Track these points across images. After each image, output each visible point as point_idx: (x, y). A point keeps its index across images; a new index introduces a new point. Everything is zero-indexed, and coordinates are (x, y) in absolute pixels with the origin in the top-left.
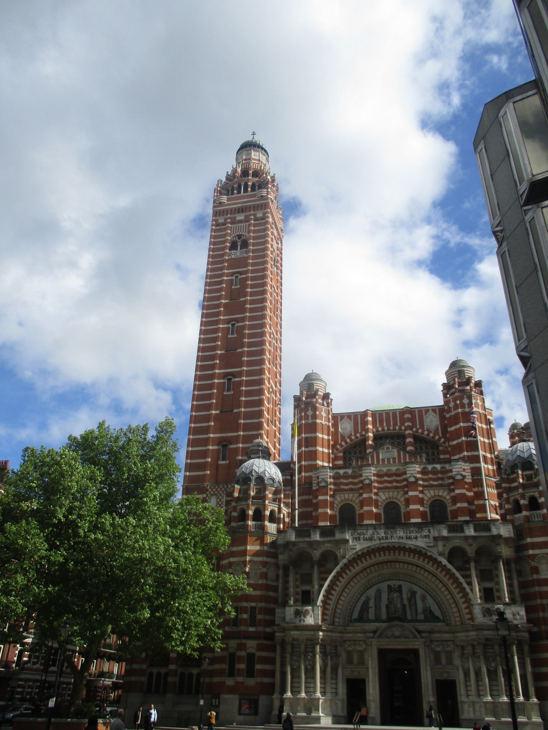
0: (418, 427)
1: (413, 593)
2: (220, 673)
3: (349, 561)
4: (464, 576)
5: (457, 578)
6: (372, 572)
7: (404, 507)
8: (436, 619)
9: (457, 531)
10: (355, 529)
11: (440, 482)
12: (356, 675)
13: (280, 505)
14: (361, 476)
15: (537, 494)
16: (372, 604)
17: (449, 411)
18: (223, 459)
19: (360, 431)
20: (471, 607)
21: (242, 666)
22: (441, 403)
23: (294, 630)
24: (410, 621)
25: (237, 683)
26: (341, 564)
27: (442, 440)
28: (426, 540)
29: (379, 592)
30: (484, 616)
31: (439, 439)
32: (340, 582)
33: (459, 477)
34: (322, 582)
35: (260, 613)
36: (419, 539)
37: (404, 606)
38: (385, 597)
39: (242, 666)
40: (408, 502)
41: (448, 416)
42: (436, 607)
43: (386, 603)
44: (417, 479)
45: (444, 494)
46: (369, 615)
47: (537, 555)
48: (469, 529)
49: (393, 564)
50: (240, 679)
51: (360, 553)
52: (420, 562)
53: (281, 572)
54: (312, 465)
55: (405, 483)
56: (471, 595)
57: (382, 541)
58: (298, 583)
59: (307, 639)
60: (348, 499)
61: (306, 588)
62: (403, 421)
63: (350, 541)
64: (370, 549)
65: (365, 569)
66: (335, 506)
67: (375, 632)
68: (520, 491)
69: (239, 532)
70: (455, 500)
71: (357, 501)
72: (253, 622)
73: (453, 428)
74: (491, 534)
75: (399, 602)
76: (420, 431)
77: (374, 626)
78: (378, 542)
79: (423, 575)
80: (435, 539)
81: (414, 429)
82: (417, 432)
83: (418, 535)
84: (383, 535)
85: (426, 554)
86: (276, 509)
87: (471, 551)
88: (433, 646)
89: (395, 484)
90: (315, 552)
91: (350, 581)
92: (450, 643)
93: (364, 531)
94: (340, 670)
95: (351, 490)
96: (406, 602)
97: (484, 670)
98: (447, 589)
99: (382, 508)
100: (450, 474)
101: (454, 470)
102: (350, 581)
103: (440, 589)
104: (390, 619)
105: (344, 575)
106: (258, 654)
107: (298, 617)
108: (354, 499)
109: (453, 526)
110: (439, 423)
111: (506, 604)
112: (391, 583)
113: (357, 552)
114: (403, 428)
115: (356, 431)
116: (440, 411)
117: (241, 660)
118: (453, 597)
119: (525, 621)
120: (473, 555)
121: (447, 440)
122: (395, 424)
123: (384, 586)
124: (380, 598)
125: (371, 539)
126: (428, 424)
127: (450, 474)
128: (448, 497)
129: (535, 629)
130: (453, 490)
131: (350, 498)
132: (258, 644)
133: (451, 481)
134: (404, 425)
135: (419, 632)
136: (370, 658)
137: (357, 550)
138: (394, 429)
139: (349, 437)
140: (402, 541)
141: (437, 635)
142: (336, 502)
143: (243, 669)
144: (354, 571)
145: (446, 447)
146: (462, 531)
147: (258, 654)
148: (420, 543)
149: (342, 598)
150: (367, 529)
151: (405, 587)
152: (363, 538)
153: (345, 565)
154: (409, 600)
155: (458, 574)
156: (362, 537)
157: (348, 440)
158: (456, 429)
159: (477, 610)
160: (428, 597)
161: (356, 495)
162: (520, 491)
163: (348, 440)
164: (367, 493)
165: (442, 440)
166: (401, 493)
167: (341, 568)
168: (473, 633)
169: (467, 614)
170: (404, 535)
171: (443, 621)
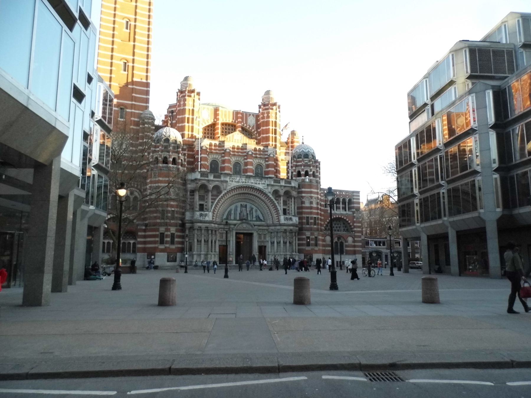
1: (252, 209)
2: (155, 242)
3: (227, 192)
4: (278, 203)
6: (235, 198)
7: (243, 166)
8: (261, 220)
9: (277, 183)
10: (231, 176)
11: (262, 156)
13: (185, 157)
14: (224, 146)
15: (309, 170)
16: (233, 212)
17: (263, 118)
18: (121, 118)
20: (279, 217)
21: (169, 239)
22: (258, 112)
23: (198, 222)
24: (250, 221)
25: (165, 247)
26: (223, 193)
27: (256, 132)
28: (264, 185)
29: (236, 207)
30: (285, 220)
31: (254, 132)
33: (272, 155)
35: (177, 213)
36: (260, 184)
37: (247, 214)
38: (239, 209)
39: (169, 239)
40: (246, 164)
41: (262, 120)
42: (262, 215)
43: (239, 212)
44: (252, 153)
45: (263, 162)
46: (231, 217)
47: (305, 196)
48: (282, 182)
49: (245, 195)
50: (167, 245)
51: (233, 188)
52: (259, 195)
53: (189, 193)
55: (245, 154)
57: (244, 184)
59: (206, 227)
60: (217, 159)
61: (202, 203)
63: (229, 182)
64: (237, 187)
65: (232, 196)
66: (208, 161)
67: (235, 225)
68: (303, 167)
69: (163, 170)
70: (268, 166)
71: (220, 160)
72: (173, 218)
73: (264, 128)
74: (291, 186)
75: (245, 212)
76: (245, 125)
77: (235, 222)
78: (241, 184)
79: (258, 201)
80: (268, 185)
81: (242, 124)
82: (243, 125)
83: (260, 183)
84: (244, 180)
85: (263, 191)
86: (183, 159)
87: (282, 192)
88: (259, 232)
89: (240, 154)
90: (210, 185)
92: (265, 231)
93: (235, 178)
94: (217, 241)
95: (217, 153)
96: (248, 212)
97: (282, 242)
98: (268, 208)
99: (232, 165)
100: (266, 153)
101: (269, 151)
104: (241, 220)
106: (176, 234)
107: (202, 217)
108: (219, 158)
109: (276, 180)
110: (255, 123)
111: (293, 216)
112: (242, 203)
113: (231, 188)
114: (237, 122)
116: (257, 116)
117: (167, 236)
119: (298, 223)
120: (283, 194)
121: (259, 134)
123: (239, 204)
124: (237, 210)
125: (238, 182)
126: (250, 122)
127: (266, 153)
128: (264, 164)
129: (300, 226)
130: (267, 161)
131: (217, 157)
132: (176, 229)
133: (266, 156)
135: (255, 226)
136: (231, 236)
137: (232, 186)
140: (252, 184)
141: (261, 227)
142: (209, 159)
143: (169, 241)
144: (228, 196)
145: (256, 136)
146: (279, 183)
147: (176, 234)
148: (261, 186)
149: (220, 209)
150: (237, 177)
151: (249, 205)
153: (225, 193)
154: (250, 212)
155: (276, 202)
156: (234, 180)
158: (266, 129)
159: (282, 218)
160: (258, 210)
161: (220, 156)
162: (303, 167)
164: (228, 157)
165: (256, 132)
166: (243, 159)
168: (278, 227)
169: (277, 219)
170: (254, 182)
171: (264, 222)
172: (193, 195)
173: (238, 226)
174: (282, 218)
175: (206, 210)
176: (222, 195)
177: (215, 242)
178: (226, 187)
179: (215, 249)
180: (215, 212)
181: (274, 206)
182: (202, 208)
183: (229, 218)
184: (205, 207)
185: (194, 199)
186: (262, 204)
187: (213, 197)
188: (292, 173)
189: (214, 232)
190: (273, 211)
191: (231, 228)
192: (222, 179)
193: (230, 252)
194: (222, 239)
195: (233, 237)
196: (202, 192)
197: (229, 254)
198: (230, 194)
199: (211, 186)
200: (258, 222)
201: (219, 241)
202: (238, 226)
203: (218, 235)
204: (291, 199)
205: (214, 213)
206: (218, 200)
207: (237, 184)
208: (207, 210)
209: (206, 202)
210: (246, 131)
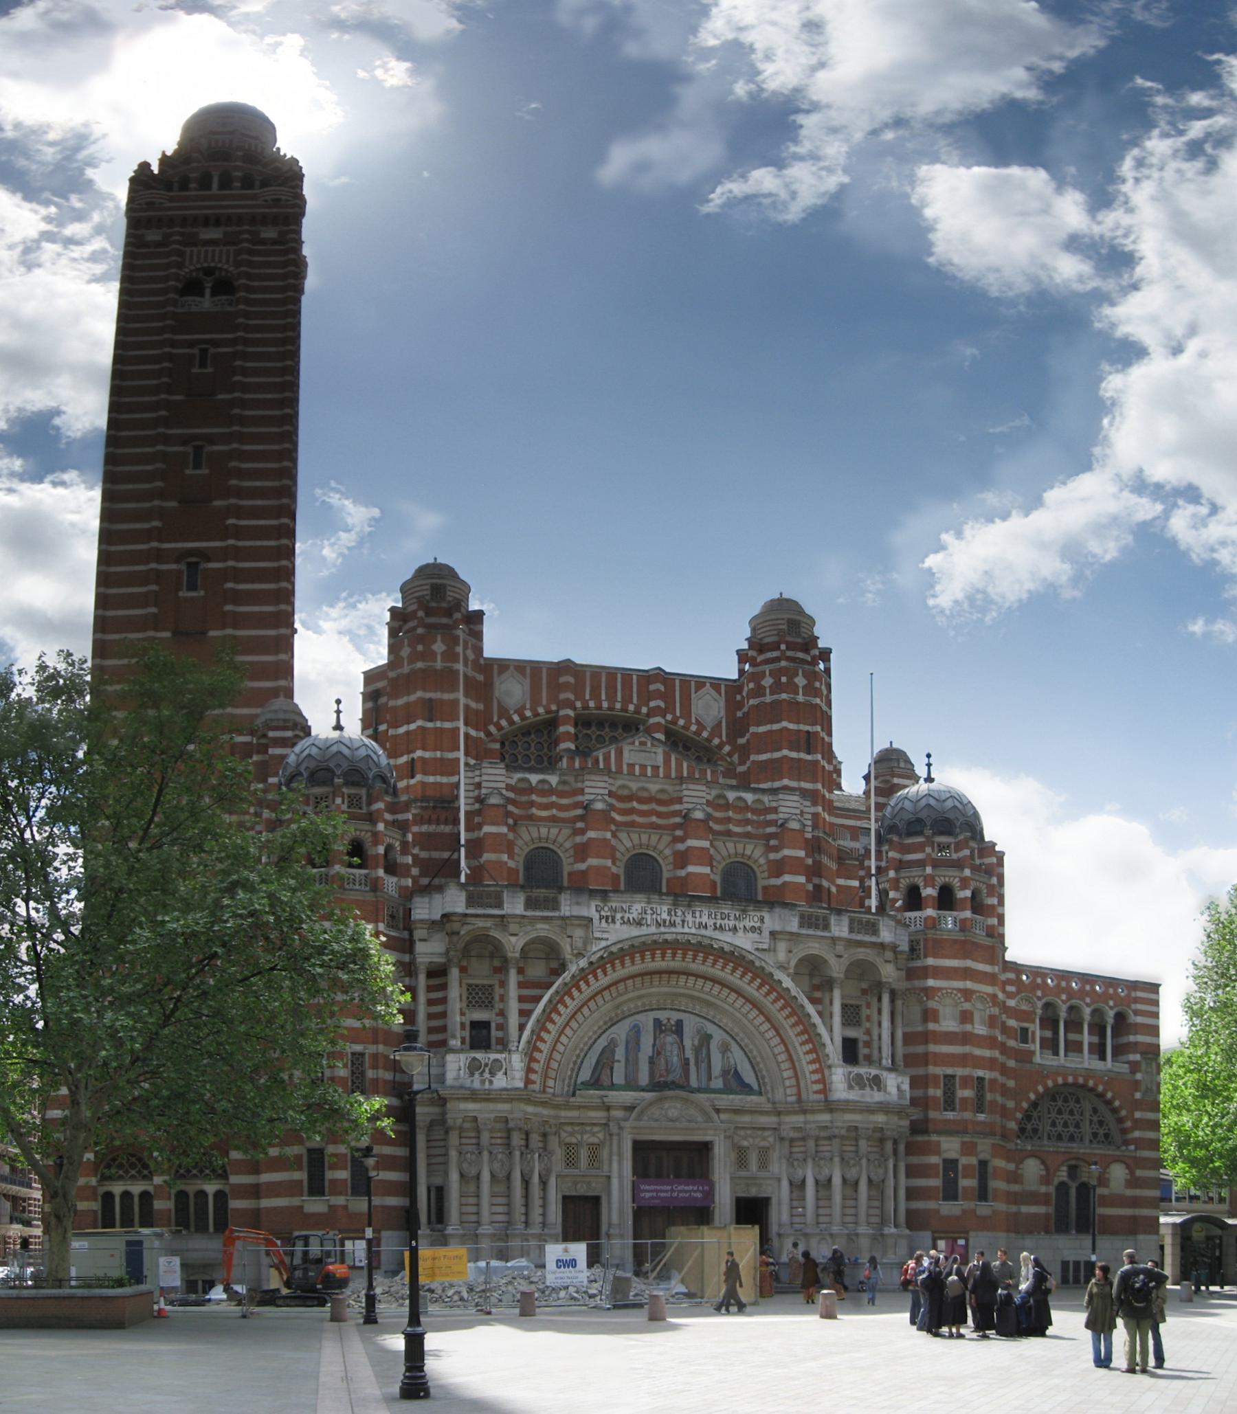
0: (678, 714)
3: (591, 963)
5: (809, 1015)
12: (582, 1190)
19: (544, 702)
26: (573, 969)
32: (566, 1007)
34: (527, 1006)
51: (614, 949)
54: (442, 759)
56: (830, 1049)
58: (464, 1004)
62: (646, 697)
65: (615, 983)
76: (681, 722)
78: (653, 929)
82: (674, 722)
90: (513, 939)
91: (582, 1007)
94: (552, 1181)
98: (779, 1034)
100: (770, 817)
102: (582, 1007)
103: (762, 1034)
105: (575, 992)
114: (644, 710)
115: (535, 702)
118: (787, 1050)
122: (627, 700)
127: (769, 817)
134: (647, 705)
135: (718, 1111)
137: (609, 943)
138: (625, 710)
139: (520, 712)
144: (595, 985)
145: (731, 763)
149: (564, 1039)
152: (622, 918)
153: (583, 969)
156: (618, 916)
157: (516, 718)
163: (516, 718)
167: (573, 976)
169: (816, 1082)
172: (444, 987)
173: (642, 1112)
174: (839, 1076)
175: (499, 1047)
176: (568, 980)
177: (544, 1183)
178: (587, 941)
179: (544, 1215)
180: (536, 1055)
181: (801, 1027)
182: (480, 1036)
183: (606, 1082)
184: (495, 1033)
185: (444, 1001)
186: (751, 1016)
187: (527, 992)
188: (883, 894)
189: (535, 1138)
190: (801, 1050)
191: (611, 1124)
192: (566, 910)
193: (610, 1225)
194: (576, 1172)
195: (620, 1162)
196: (481, 972)
197: (609, 1236)
198: (605, 974)
199: (513, 944)
200: (731, 1097)
201: (557, 1177)
202: (642, 1112)
203: (558, 1154)
204: (880, 1000)
205: (532, 1059)
206: (550, 1001)
207: (635, 931)
208: (504, 1045)
209: (502, 1013)
210: (687, 748)
